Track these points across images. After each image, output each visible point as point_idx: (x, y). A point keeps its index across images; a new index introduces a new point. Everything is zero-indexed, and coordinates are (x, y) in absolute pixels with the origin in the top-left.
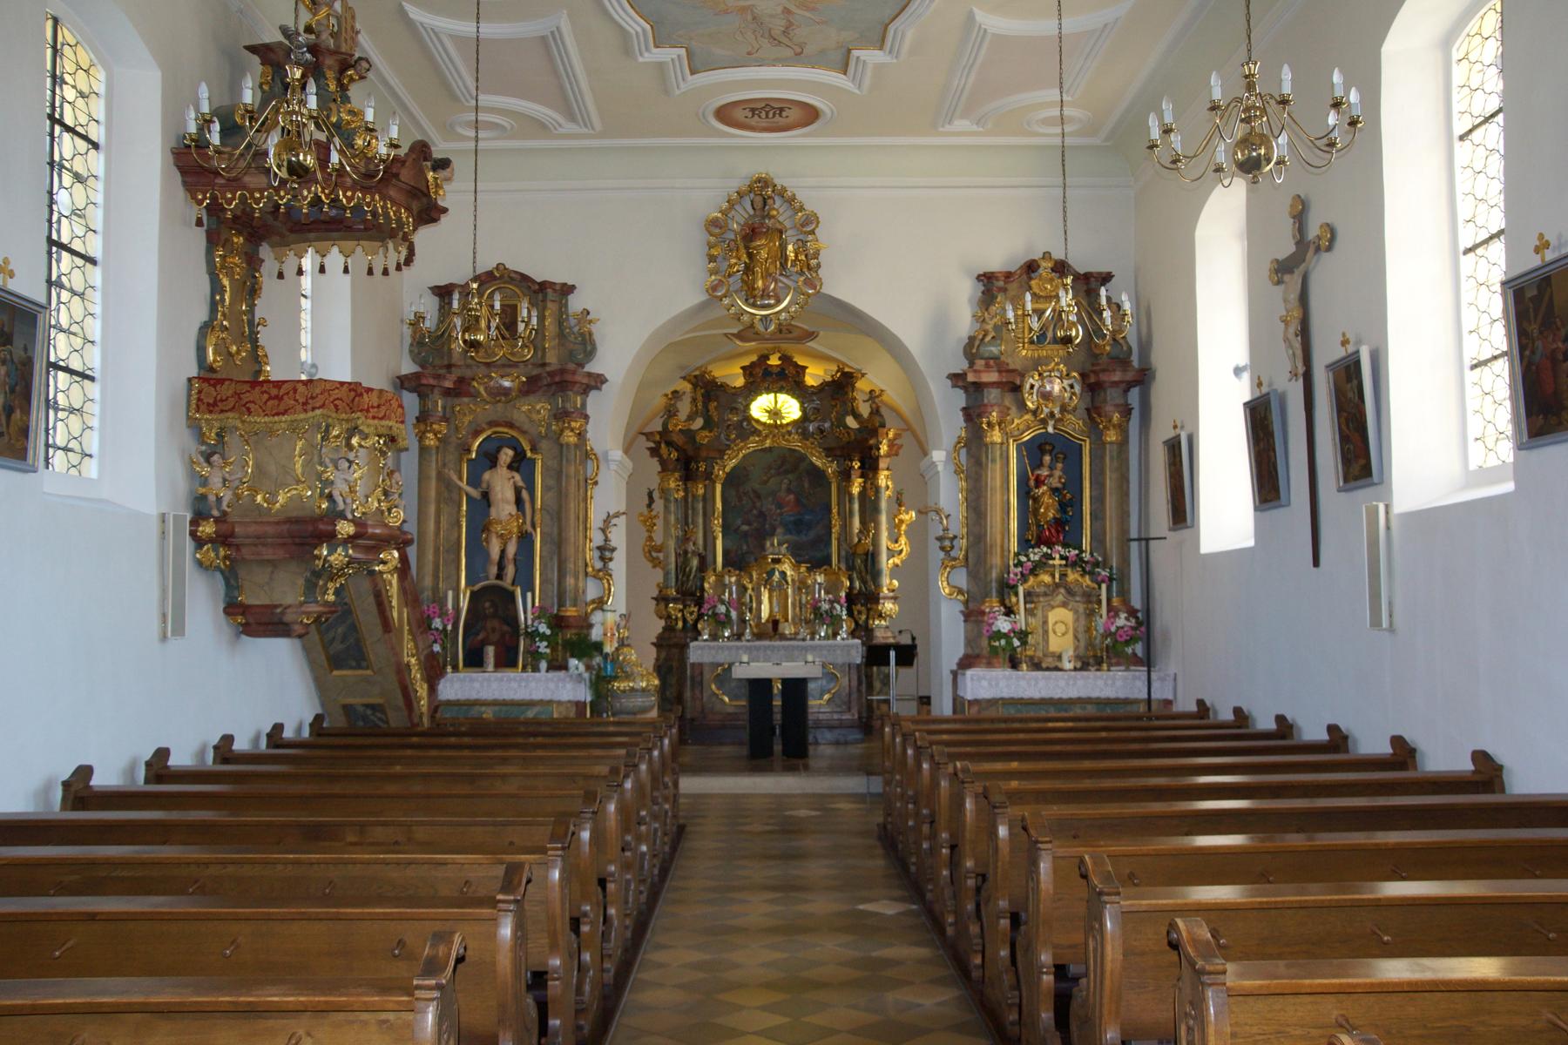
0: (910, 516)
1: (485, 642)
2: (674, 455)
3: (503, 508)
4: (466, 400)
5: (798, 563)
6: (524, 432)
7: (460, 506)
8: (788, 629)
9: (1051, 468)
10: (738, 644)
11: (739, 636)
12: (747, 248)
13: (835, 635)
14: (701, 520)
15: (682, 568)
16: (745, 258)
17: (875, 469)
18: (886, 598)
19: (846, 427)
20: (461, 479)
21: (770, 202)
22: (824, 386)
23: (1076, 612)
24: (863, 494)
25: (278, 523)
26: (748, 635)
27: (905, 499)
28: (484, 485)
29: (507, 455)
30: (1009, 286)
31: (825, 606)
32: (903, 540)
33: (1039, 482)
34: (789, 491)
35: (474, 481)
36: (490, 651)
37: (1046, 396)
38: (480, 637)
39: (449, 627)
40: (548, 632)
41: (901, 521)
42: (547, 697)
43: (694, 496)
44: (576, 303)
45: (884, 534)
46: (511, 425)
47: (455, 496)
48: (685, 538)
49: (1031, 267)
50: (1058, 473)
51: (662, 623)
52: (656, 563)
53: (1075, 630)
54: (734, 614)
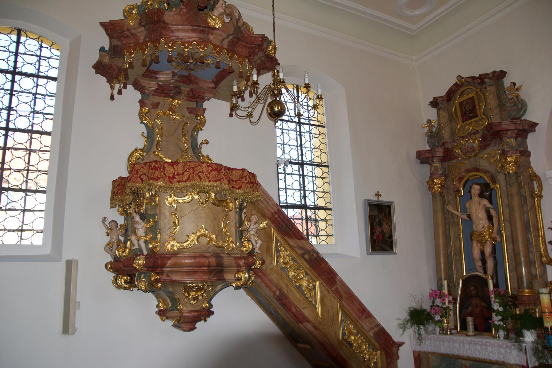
4: (455, 161)
6: (486, 172)
7: (459, 225)
29: (476, 189)
38: (469, 310)
40: (501, 309)
42: (501, 359)
46: (478, 170)
47: (456, 220)
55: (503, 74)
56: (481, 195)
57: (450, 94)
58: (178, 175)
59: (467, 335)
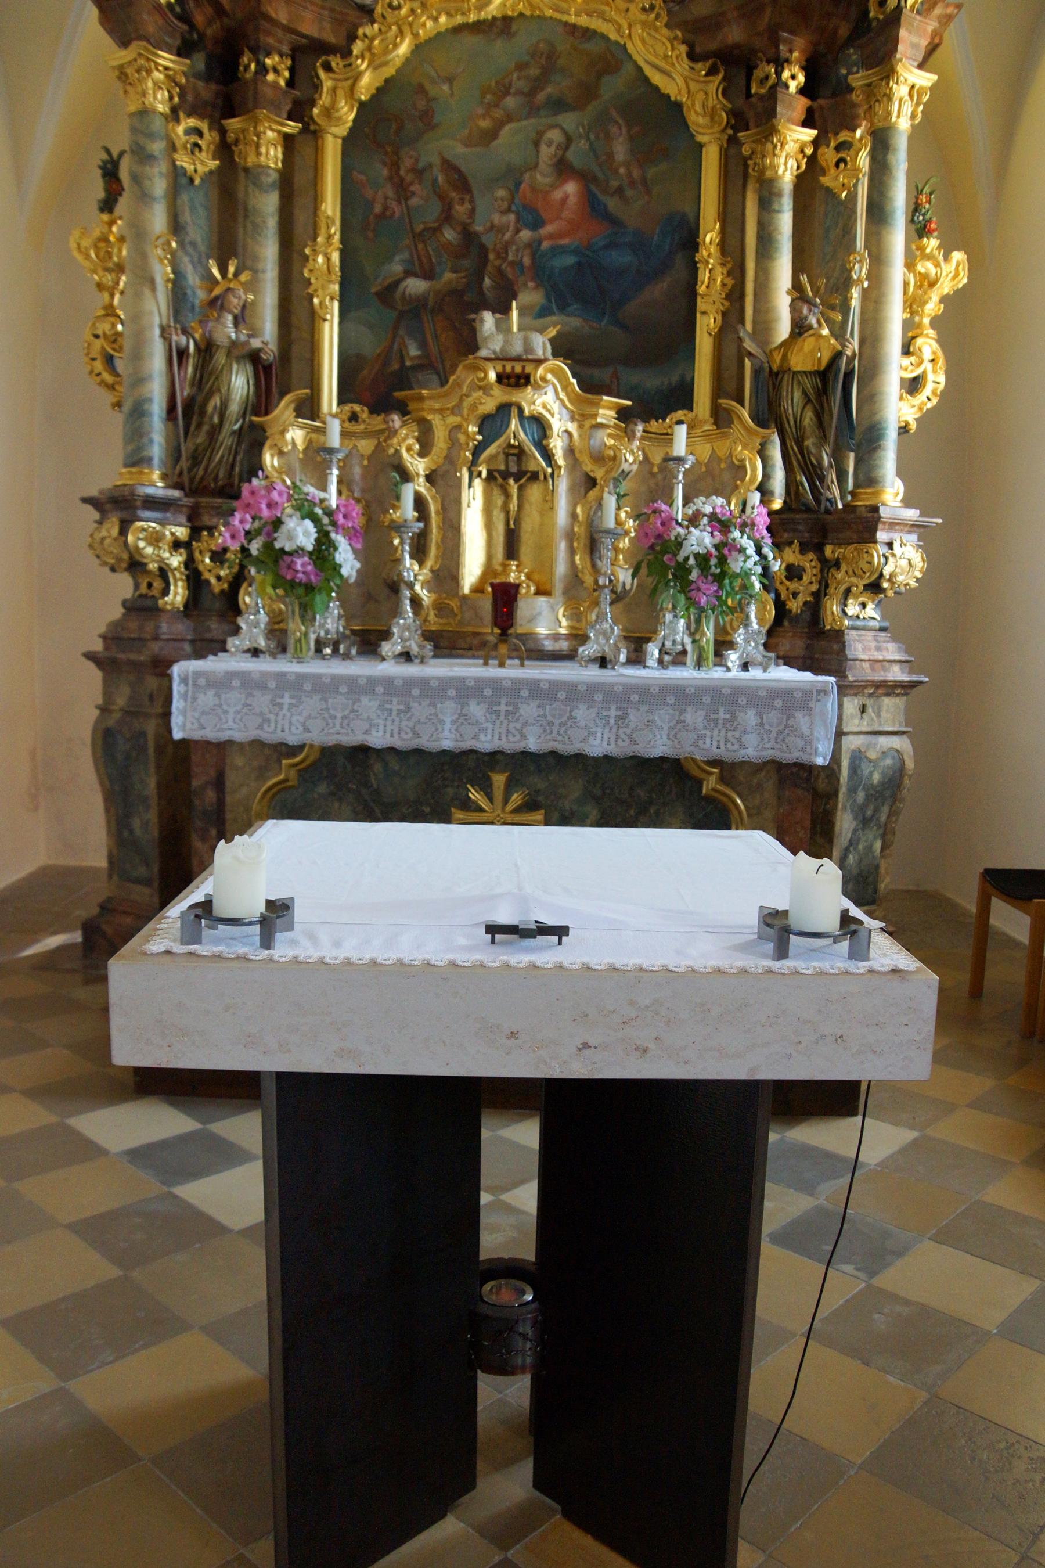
0: (951, 272)
5: (592, 387)
8: (545, 619)
10: (361, 668)
11: (369, 641)
13: (723, 645)
14: (269, 251)
15: (188, 412)
18: (893, 525)
26: (404, 631)
34: (563, 168)
51: (124, 586)
54: (347, 560)
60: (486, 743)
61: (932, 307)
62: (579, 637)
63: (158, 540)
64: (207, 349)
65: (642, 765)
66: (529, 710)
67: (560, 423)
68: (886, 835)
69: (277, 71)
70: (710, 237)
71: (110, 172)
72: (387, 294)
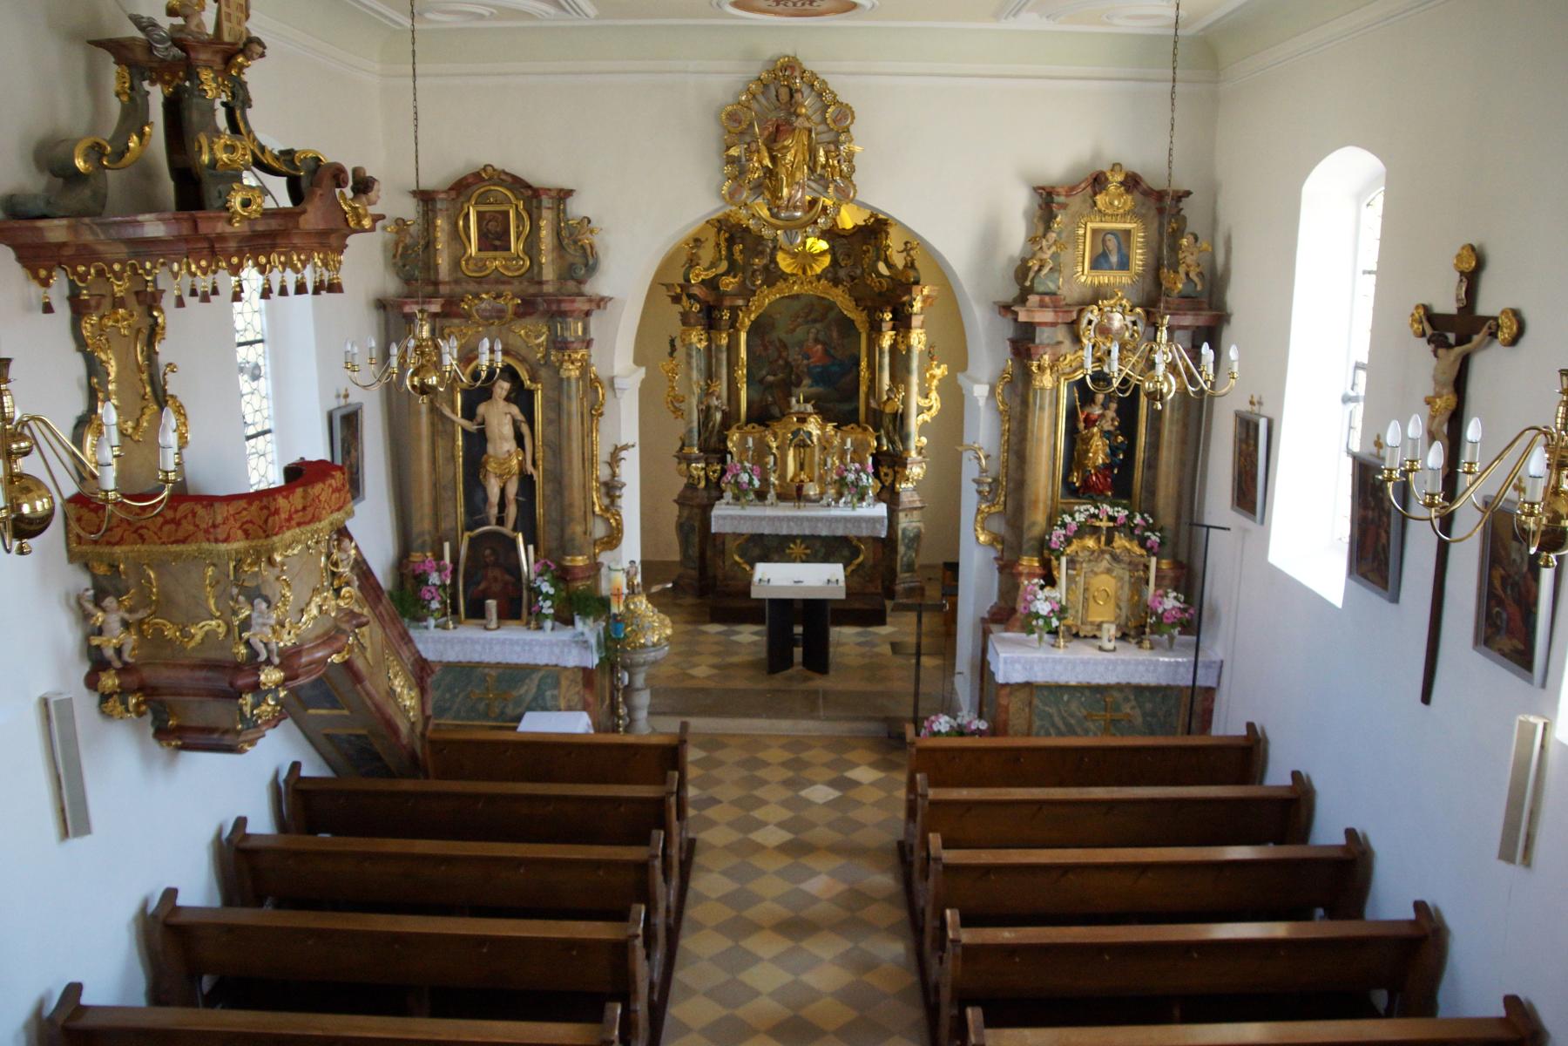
0: (940, 371)
1: (487, 595)
2: (696, 307)
3: (502, 442)
4: (456, 321)
7: (454, 440)
8: (812, 490)
9: (1105, 406)
11: (761, 495)
12: (770, 150)
14: (724, 371)
16: (767, 162)
17: (908, 327)
19: (879, 275)
20: (454, 411)
21: (798, 96)
22: (858, 229)
23: (1121, 579)
24: (893, 347)
25: (193, 667)
27: (936, 352)
28: (479, 419)
29: (502, 388)
30: (1070, 200)
31: (851, 477)
32: (934, 395)
33: (1090, 422)
34: (817, 341)
35: (469, 413)
36: (492, 604)
37: (1104, 330)
38: (482, 586)
39: (448, 582)
40: (552, 591)
41: (933, 377)
43: (719, 347)
44: (576, 208)
45: (915, 389)
48: (707, 393)
49: (1098, 182)
50: (1111, 414)
52: (677, 412)
53: (1118, 598)
54: (757, 483)
55: (569, 193)
56: (507, 399)
57: (463, 187)
58: (297, 511)
59: (486, 628)
60: (795, 532)
61: (935, 382)
62: (822, 494)
63: (697, 468)
64: (708, 408)
65: (836, 538)
66: (806, 524)
67: (816, 432)
68: (917, 551)
69: (726, 315)
70: (864, 364)
71: (672, 342)
72: (761, 381)
